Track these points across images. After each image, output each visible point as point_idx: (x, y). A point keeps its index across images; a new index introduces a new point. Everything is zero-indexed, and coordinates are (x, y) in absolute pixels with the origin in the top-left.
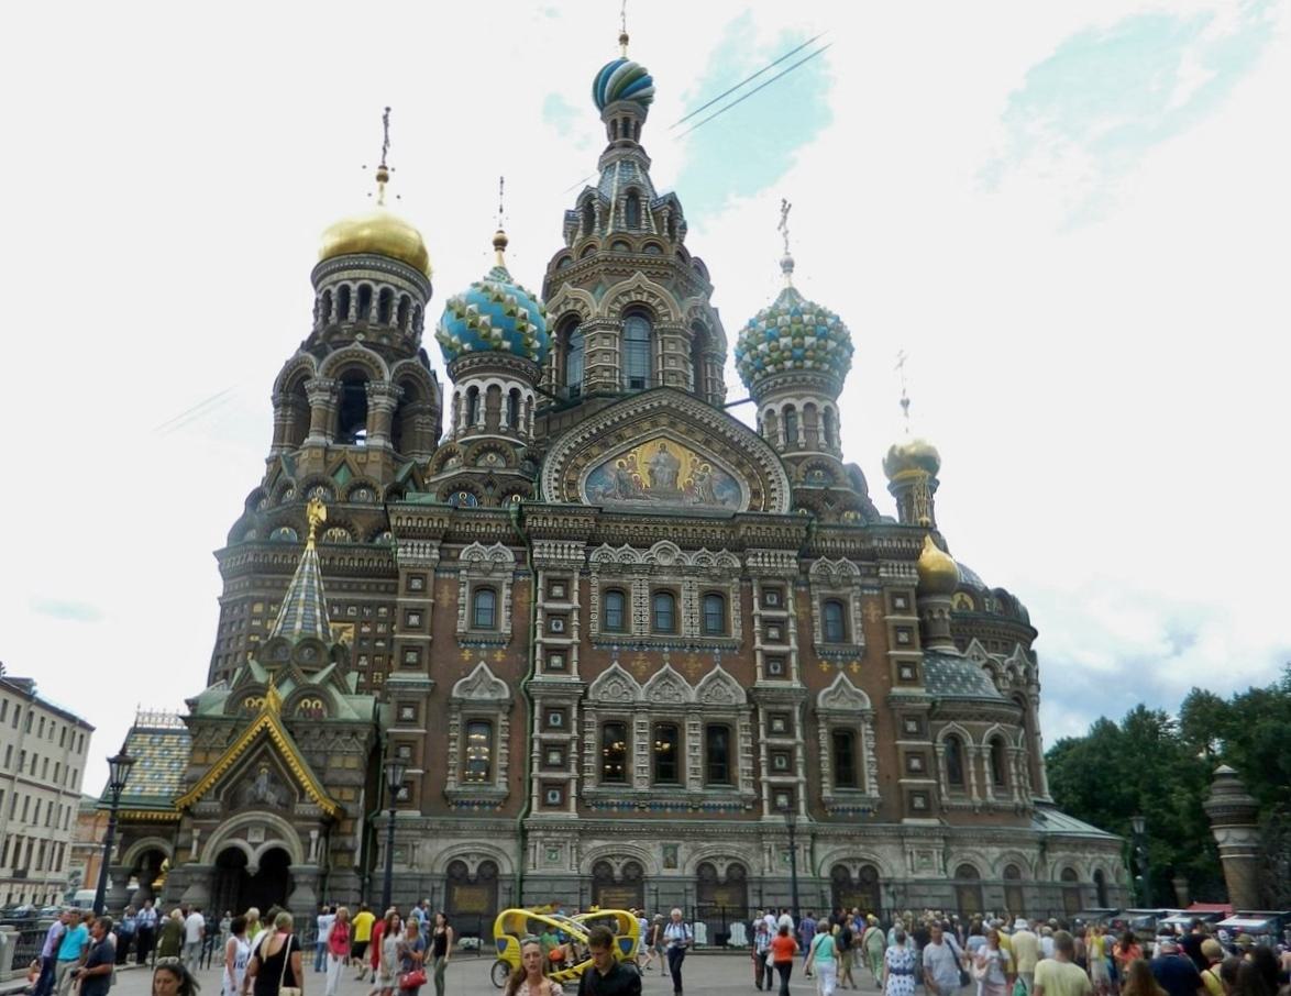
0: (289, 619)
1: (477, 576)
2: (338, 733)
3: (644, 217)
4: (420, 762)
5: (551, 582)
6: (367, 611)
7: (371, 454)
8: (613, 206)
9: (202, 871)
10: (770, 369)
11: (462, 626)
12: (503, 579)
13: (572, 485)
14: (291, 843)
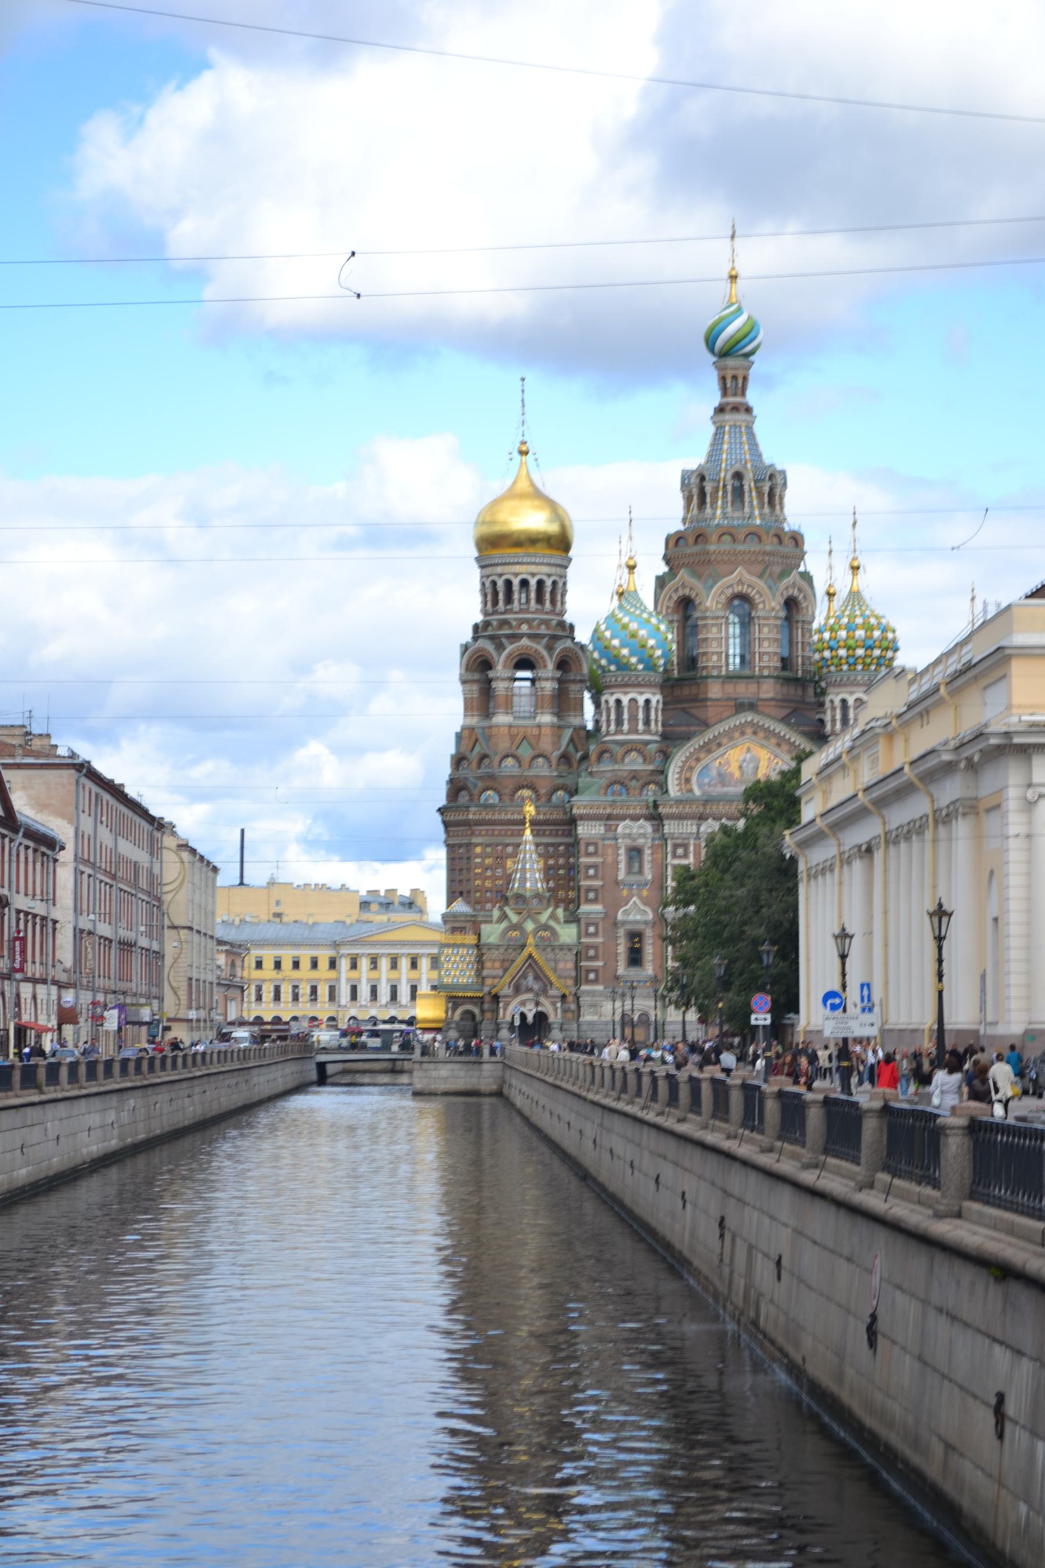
0: (523, 880)
1: (628, 842)
2: (561, 950)
3: (747, 499)
4: (601, 957)
5: (676, 846)
6: (551, 849)
7: (543, 730)
8: (721, 484)
9: (506, 1022)
10: (832, 668)
11: (622, 875)
12: (645, 843)
13: (688, 780)
14: (547, 1007)
